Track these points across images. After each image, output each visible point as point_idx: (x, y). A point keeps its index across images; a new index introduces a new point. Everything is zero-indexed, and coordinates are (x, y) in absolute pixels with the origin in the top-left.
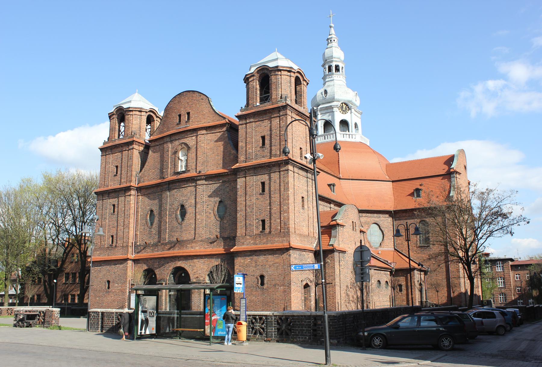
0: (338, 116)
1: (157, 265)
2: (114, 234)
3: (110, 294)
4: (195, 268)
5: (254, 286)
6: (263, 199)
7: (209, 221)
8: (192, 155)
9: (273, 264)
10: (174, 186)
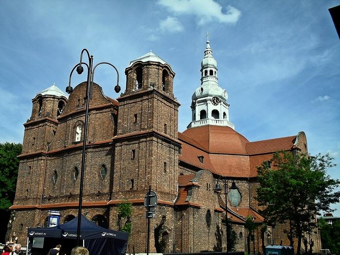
0: (211, 107)
7: (94, 180)
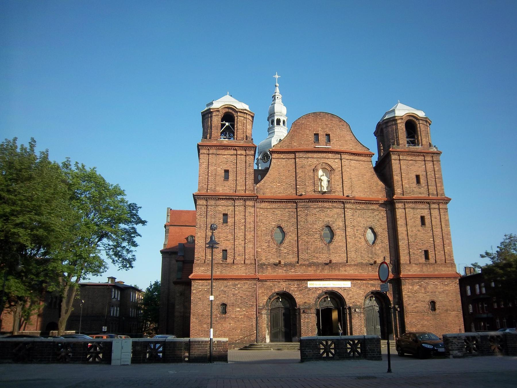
1: (296, 288)
2: (227, 249)
3: (227, 320)
5: (426, 311)
6: (424, 231)
7: (360, 246)
8: (337, 176)
9: (443, 292)
10: (316, 205)
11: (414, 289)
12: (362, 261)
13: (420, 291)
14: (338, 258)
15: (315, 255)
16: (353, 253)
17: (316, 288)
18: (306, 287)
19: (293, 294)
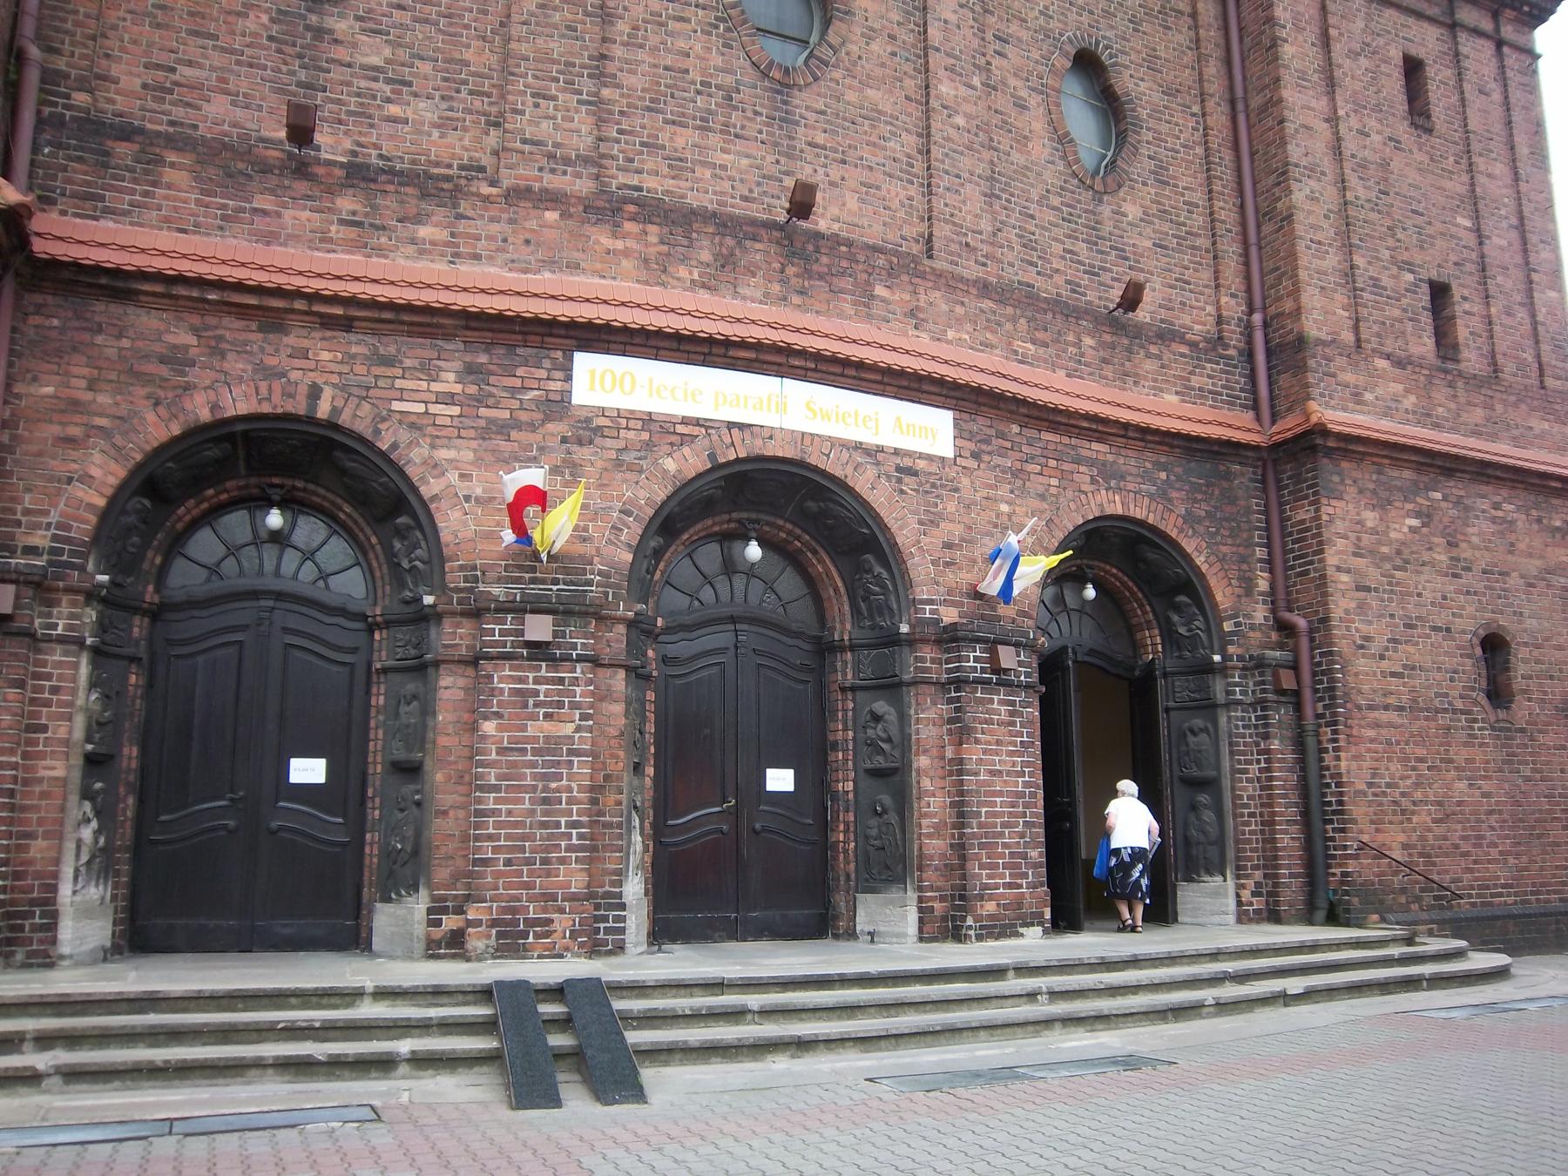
1: (448, 399)
4: (951, 507)
5: (1459, 704)
11: (1393, 535)
12: (1030, 276)
13: (1426, 557)
14: (852, 203)
15: (663, 138)
16: (973, 193)
17: (648, 420)
18: (558, 406)
19: (415, 458)
